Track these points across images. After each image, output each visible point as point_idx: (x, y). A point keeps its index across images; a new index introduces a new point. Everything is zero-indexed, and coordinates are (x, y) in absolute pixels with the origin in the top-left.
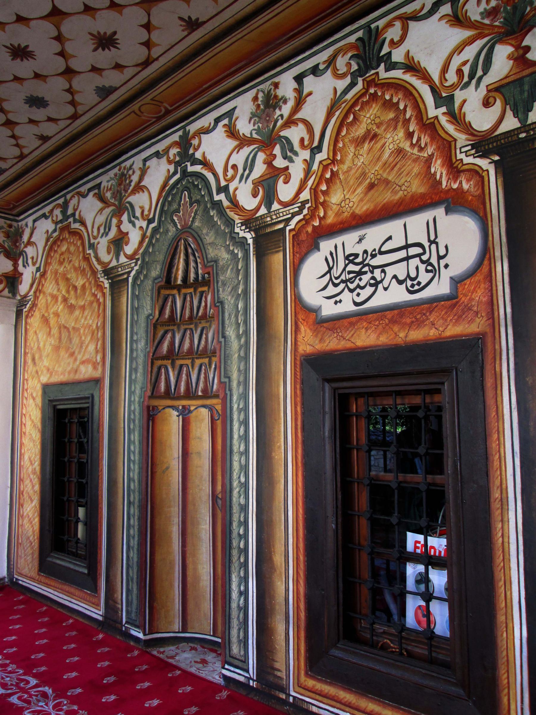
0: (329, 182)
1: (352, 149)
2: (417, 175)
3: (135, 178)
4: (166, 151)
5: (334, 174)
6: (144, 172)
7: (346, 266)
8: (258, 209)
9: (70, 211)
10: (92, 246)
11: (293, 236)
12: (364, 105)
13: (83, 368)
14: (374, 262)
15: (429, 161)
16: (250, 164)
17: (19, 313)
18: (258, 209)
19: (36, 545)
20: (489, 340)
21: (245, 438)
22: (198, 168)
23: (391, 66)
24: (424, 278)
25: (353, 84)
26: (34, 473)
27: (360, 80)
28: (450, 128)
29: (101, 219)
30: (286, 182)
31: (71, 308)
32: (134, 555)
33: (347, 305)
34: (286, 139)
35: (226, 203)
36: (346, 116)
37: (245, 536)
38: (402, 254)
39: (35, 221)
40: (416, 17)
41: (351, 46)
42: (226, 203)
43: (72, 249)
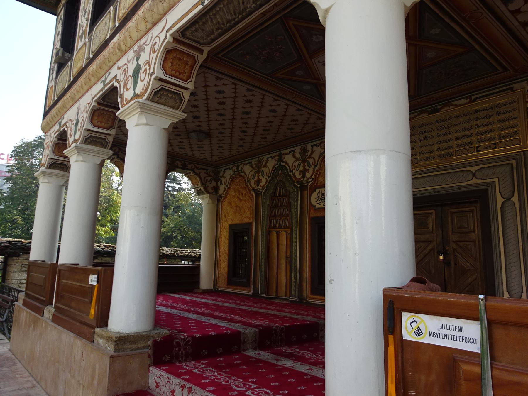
0: (319, 175)
3: (264, 163)
4: (274, 157)
6: (267, 162)
8: (301, 178)
9: (240, 169)
10: (248, 181)
13: (245, 219)
16: (299, 166)
17: (218, 201)
18: (301, 178)
19: (226, 276)
21: (296, 238)
22: (284, 164)
26: (226, 253)
29: (252, 173)
30: (308, 173)
31: (241, 200)
32: (263, 273)
35: (292, 176)
37: (296, 263)
39: (225, 170)
42: (292, 176)
43: (241, 181)
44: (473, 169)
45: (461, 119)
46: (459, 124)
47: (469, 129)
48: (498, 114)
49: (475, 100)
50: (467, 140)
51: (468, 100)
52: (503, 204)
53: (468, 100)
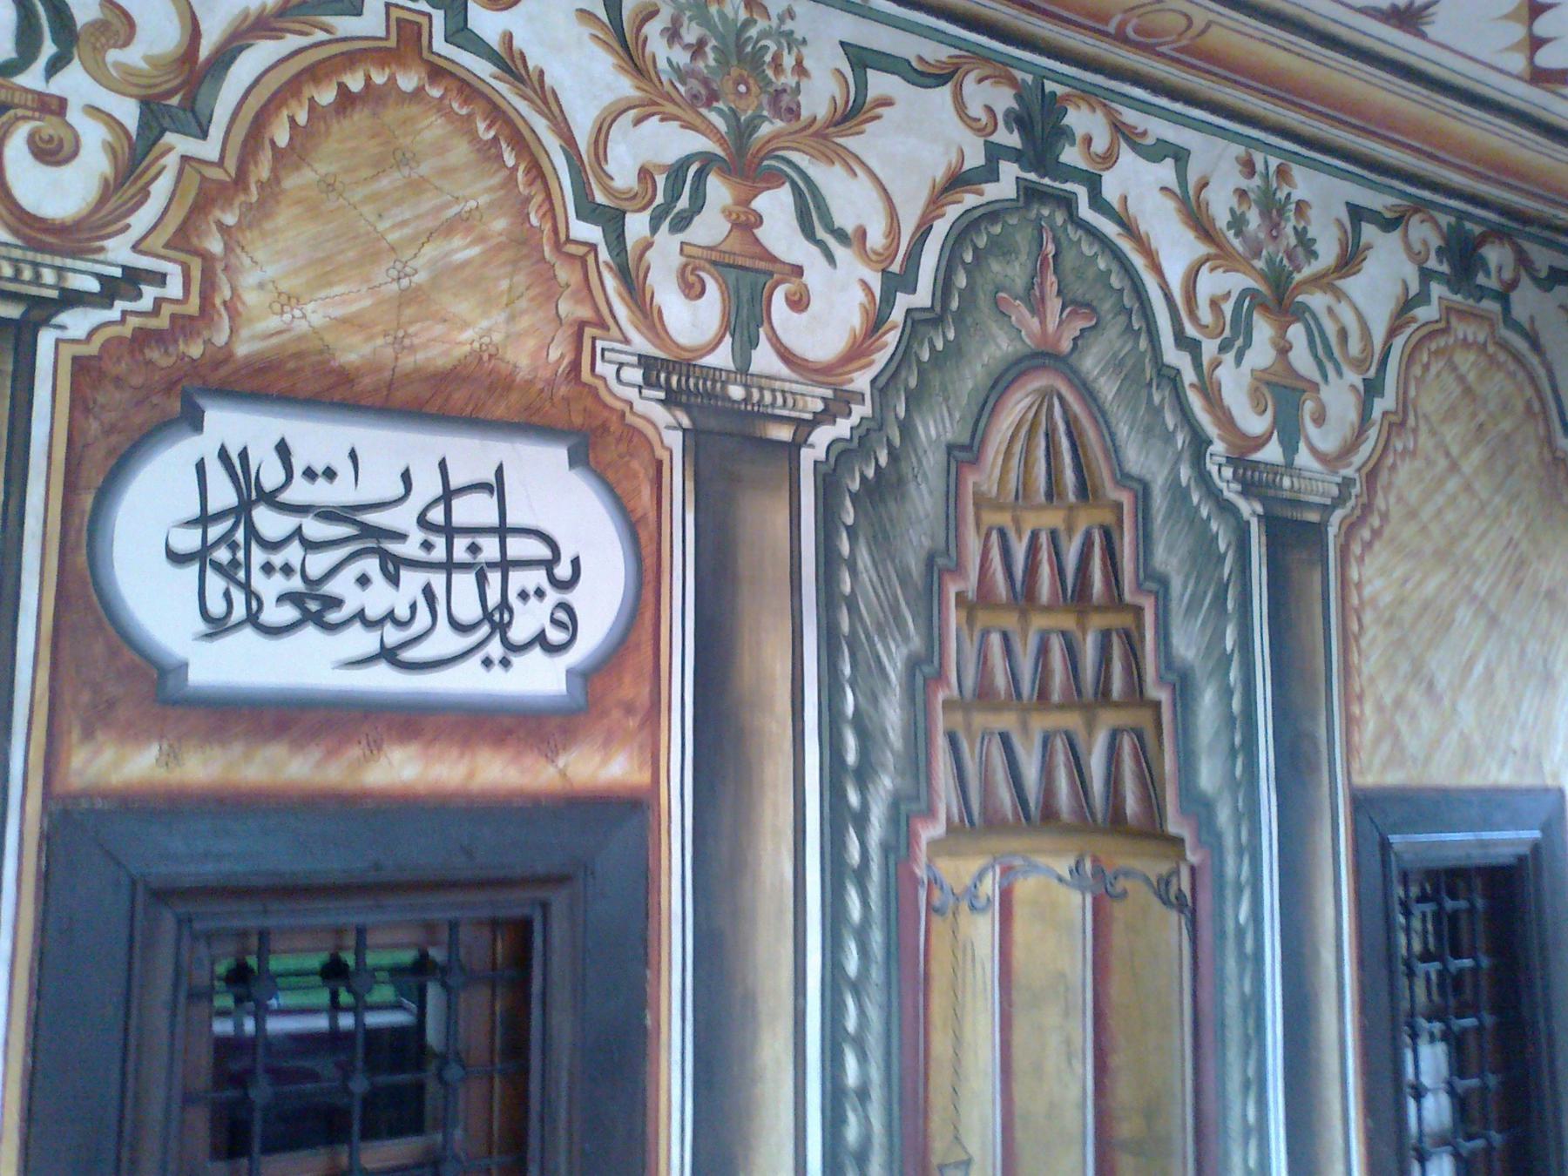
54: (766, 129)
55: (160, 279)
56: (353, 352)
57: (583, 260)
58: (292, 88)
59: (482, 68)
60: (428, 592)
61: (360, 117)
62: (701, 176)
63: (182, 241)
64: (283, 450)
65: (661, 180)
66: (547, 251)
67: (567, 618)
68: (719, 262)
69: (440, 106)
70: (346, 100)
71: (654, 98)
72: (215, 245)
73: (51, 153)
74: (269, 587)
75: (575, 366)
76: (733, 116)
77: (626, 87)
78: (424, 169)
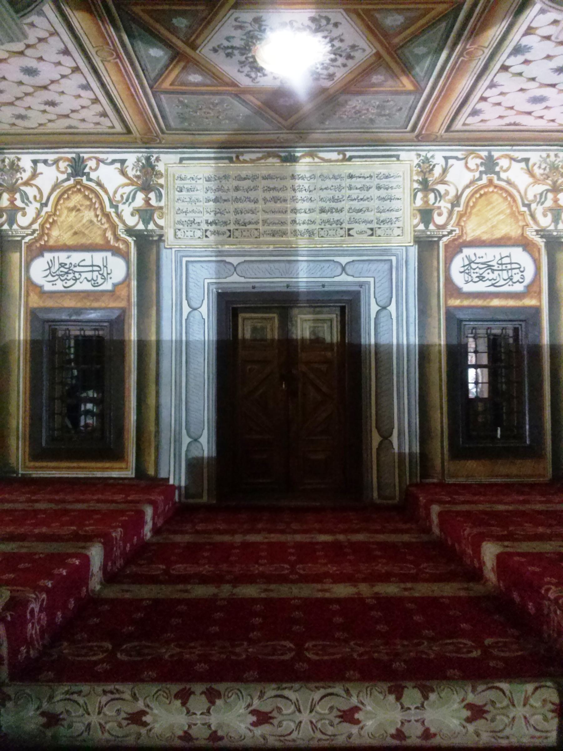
1: (65, 212)
2: (100, 235)
5: (54, 221)
7: (59, 268)
11: (27, 247)
12: (73, 192)
14: (75, 269)
15: (105, 230)
20: (127, 311)
23: (89, 180)
24: (100, 281)
25: (68, 179)
27: (72, 179)
28: (116, 220)
33: (59, 286)
34: (25, 192)
36: (63, 194)
38: (90, 269)
40: (103, 161)
41: (67, 159)
44: (343, 260)
45: (329, 183)
46: (326, 189)
47: (339, 200)
48: (379, 188)
49: (350, 158)
50: (336, 216)
51: (341, 157)
52: (378, 313)
53: (341, 157)
54: (560, 181)
55: (455, 231)
56: (485, 237)
57: (523, 215)
58: (472, 196)
59: (503, 184)
60: (499, 275)
61: (483, 198)
62: (546, 194)
63: (458, 224)
64: (475, 254)
65: (538, 196)
66: (517, 214)
67: (523, 277)
68: (551, 209)
69: (497, 193)
70: (481, 196)
71: (537, 181)
72: (463, 224)
73: (440, 215)
74: (474, 276)
75: (523, 234)
76: (552, 181)
77: (531, 180)
78: (494, 204)
